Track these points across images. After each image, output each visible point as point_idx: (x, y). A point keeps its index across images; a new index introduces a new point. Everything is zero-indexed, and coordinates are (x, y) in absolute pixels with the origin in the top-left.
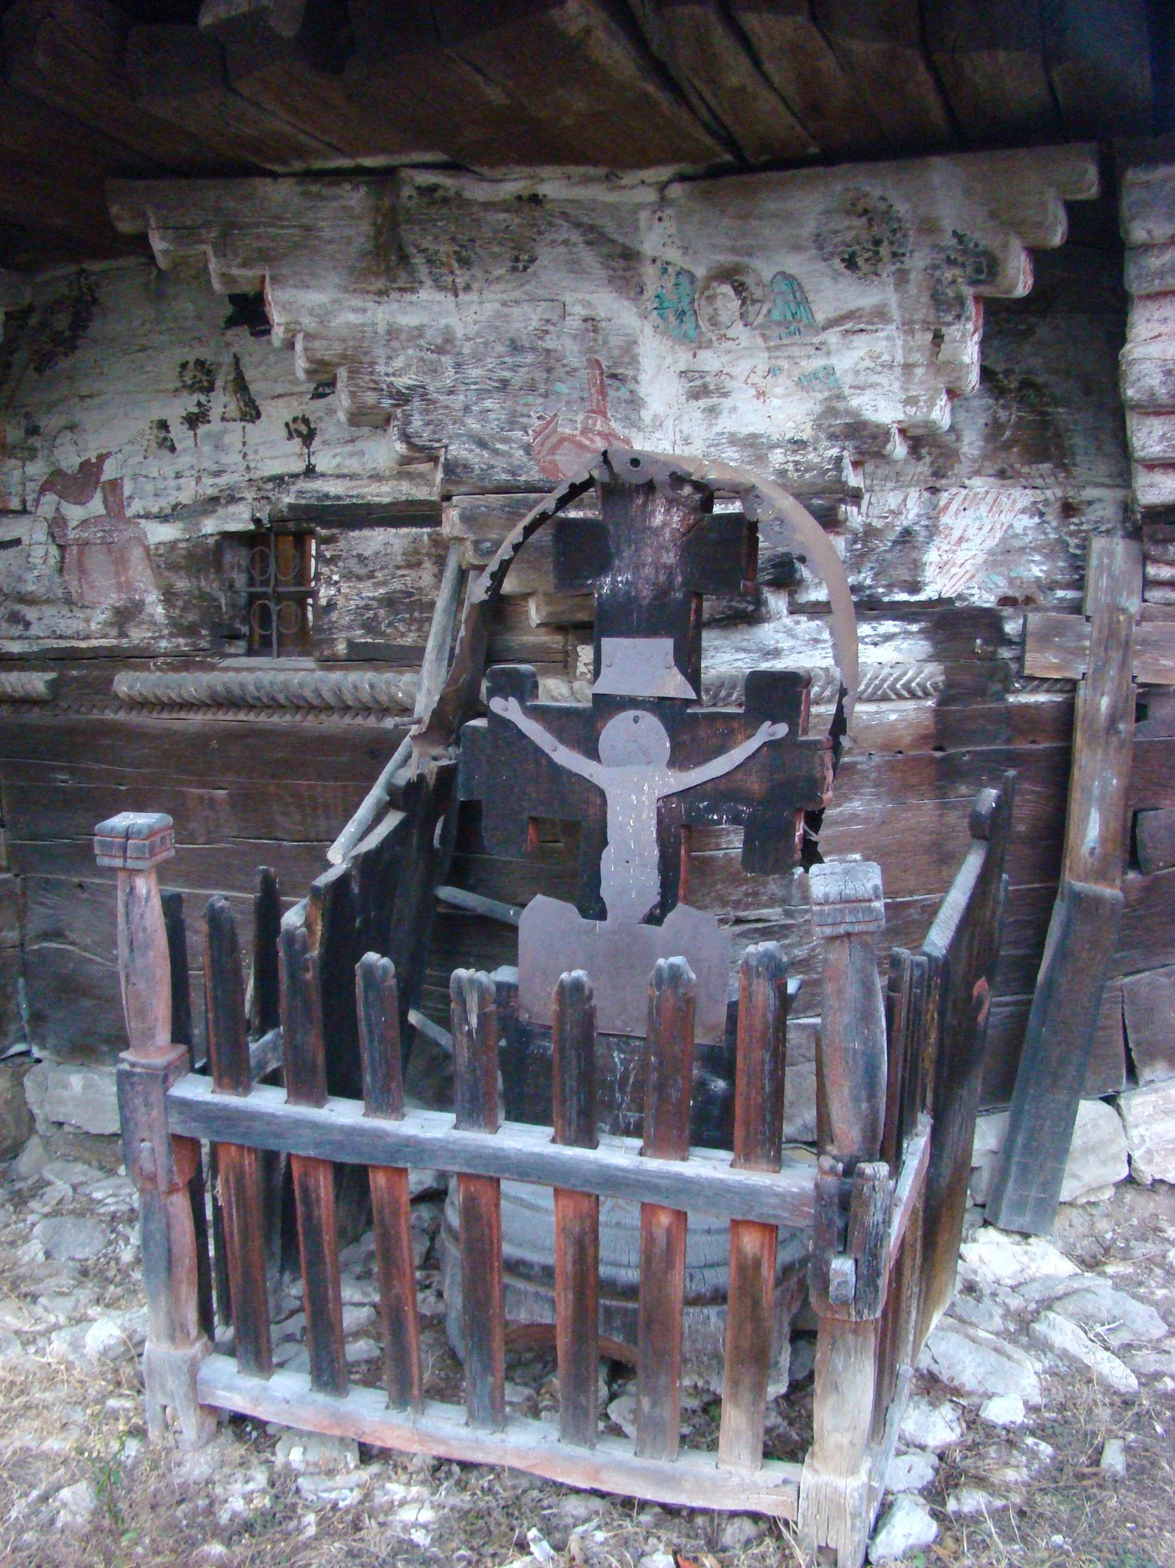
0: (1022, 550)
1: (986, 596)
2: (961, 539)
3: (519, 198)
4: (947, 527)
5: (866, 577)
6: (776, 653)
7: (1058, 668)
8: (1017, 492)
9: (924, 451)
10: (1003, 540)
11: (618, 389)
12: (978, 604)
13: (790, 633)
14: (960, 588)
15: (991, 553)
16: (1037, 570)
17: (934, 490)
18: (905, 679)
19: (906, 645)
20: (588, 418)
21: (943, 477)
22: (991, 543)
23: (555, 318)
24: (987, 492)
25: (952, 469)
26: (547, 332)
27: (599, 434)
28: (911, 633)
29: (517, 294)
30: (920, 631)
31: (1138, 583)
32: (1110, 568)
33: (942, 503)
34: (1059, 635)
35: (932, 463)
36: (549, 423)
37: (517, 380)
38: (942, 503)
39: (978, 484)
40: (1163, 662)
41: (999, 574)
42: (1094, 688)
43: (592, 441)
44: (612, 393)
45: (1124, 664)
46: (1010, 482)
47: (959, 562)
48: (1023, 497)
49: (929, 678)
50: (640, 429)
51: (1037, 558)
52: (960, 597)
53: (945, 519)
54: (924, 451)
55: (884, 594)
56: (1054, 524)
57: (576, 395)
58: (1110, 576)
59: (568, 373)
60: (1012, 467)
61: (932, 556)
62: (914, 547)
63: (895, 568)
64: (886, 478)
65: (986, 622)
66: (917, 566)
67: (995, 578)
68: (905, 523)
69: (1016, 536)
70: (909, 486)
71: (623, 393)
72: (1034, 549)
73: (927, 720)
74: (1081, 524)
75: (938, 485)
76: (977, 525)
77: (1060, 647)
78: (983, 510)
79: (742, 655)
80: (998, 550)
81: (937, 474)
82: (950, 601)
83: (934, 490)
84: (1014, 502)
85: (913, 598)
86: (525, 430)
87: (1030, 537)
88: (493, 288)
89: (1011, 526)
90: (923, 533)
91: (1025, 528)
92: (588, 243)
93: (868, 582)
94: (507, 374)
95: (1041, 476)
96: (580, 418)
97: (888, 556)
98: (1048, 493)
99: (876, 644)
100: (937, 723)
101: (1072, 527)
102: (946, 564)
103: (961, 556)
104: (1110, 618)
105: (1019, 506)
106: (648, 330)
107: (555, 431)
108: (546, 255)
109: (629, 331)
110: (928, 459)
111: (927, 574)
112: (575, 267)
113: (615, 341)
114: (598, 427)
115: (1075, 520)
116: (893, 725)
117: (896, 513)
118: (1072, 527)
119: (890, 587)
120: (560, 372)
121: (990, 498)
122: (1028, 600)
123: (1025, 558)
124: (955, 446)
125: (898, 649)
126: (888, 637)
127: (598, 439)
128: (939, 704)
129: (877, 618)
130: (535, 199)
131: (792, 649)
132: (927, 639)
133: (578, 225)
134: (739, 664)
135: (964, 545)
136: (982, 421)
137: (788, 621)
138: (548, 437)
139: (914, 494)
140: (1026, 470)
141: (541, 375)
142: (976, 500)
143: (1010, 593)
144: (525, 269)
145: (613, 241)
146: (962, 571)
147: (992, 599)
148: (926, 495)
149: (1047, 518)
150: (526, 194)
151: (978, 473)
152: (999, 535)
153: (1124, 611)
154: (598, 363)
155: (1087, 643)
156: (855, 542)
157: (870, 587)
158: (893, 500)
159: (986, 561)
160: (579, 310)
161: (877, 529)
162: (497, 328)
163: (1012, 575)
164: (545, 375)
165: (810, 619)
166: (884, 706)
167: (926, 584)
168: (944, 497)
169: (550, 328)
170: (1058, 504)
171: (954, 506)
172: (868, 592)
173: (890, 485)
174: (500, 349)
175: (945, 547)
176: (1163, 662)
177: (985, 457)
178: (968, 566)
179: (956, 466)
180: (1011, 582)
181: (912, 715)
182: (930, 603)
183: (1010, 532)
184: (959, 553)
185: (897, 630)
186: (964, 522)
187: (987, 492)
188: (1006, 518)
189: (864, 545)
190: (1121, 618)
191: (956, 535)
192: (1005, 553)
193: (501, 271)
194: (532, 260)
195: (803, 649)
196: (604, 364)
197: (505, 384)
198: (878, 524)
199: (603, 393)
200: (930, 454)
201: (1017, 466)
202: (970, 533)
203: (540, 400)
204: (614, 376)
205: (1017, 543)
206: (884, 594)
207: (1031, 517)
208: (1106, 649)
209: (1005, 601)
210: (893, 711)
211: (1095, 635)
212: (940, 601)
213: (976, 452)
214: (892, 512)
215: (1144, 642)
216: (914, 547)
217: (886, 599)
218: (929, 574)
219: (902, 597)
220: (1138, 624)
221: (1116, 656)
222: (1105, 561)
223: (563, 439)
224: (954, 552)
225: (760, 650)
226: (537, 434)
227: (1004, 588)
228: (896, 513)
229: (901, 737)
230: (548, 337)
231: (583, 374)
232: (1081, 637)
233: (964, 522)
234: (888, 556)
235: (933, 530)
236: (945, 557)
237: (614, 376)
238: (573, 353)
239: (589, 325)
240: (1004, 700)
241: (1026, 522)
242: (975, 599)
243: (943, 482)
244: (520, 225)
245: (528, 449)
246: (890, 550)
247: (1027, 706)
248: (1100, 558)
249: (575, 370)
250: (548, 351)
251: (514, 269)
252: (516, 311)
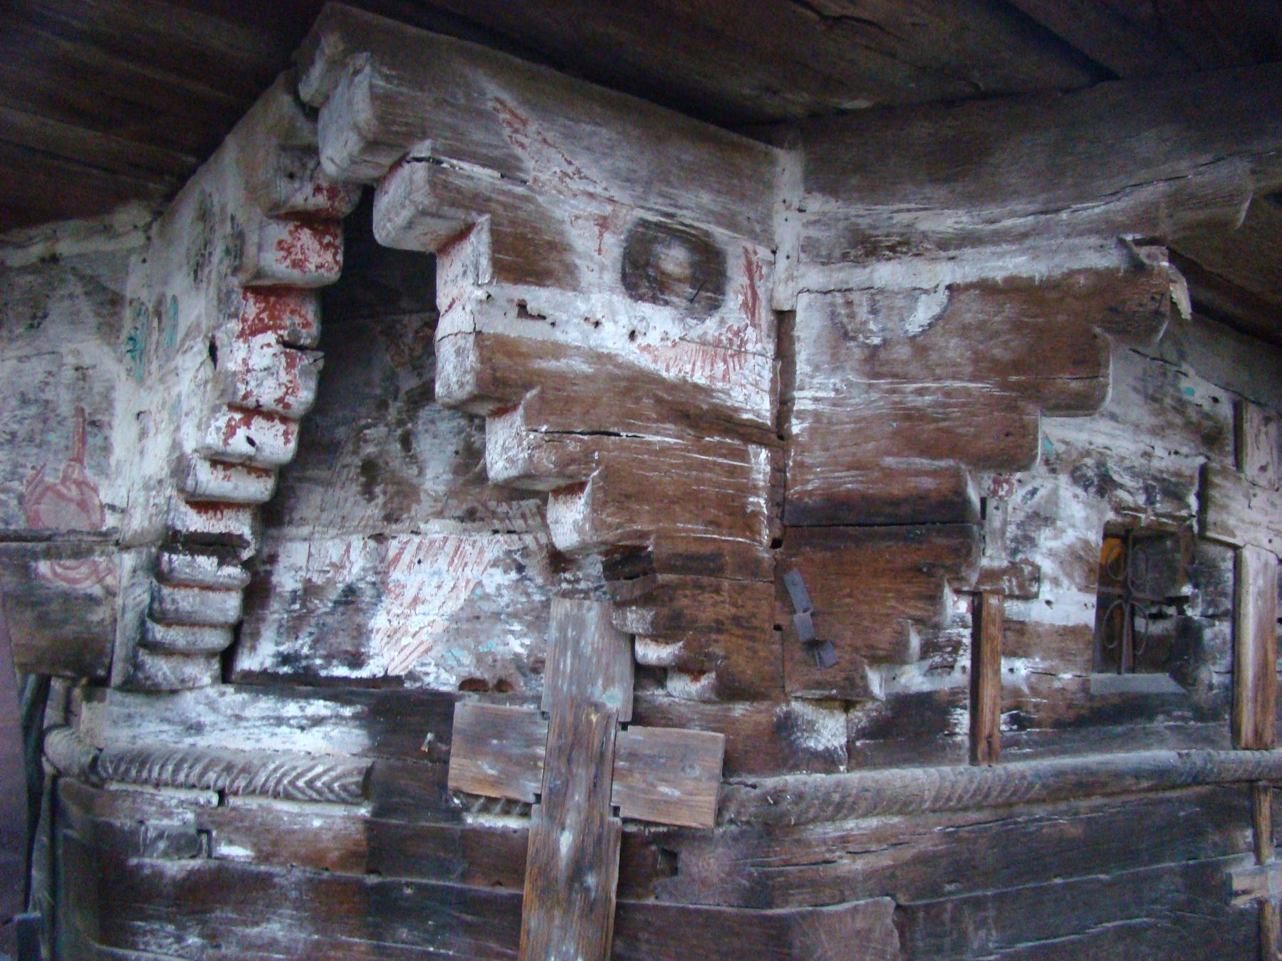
0: (496, 616)
1: (444, 676)
2: (416, 601)
3: (43, 260)
4: (398, 584)
5: (302, 645)
6: (198, 728)
7: (495, 782)
8: (484, 539)
9: (378, 490)
10: (470, 602)
11: (96, 435)
12: (434, 686)
13: (212, 705)
14: (412, 664)
15: (454, 618)
16: (517, 645)
17: (380, 538)
18: (310, 775)
19: (336, 732)
20: (69, 466)
21: (396, 521)
22: (453, 606)
23: (54, 369)
24: (446, 539)
25: (409, 509)
26: (47, 384)
27: (75, 482)
28: (342, 718)
29: (28, 350)
30: (355, 717)
31: (623, 669)
32: (577, 642)
33: (391, 554)
34: (500, 736)
35: (385, 504)
36: (39, 472)
37: (22, 431)
38: (391, 554)
39: (435, 529)
40: (664, 789)
41: (465, 648)
42: (551, 817)
43: (69, 489)
44: (90, 440)
45: (594, 788)
46: (477, 524)
47: (412, 631)
48: (495, 546)
49: (337, 778)
50: (107, 476)
51: (517, 627)
52: (411, 676)
53: (396, 575)
54: (378, 490)
55: (322, 667)
56: (540, 581)
57: (63, 443)
58: (577, 654)
59: (59, 423)
60: (485, 505)
61: (379, 621)
62: (358, 610)
63: (336, 635)
64: (331, 524)
65: (437, 707)
66: (361, 633)
67: (456, 652)
68: (349, 580)
69: (486, 597)
70: (351, 534)
71: (99, 441)
72: (515, 616)
73: (356, 831)
74: (578, 581)
75: (387, 532)
76: (434, 583)
77: (499, 755)
78: (442, 562)
79: (165, 727)
80: (463, 615)
81: (390, 518)
82: (398, 680)
83: (380, 538)
84: (481, 551)
85: (355, 674)
86: (21, 479)
87: (506, 600)
88: (14, 346)
89: (479, 584)
90: (370, 592)
91: (499, 587)
92: (87, 294)
93: (305, 651)
94: (15, 427)
95: (523, 516)
96: (62, 467)
97: (330, 620)
98: (528, 539)
99: (302, 728)
100: (369, 839)
101: (564, 586)
102: (396, 632)
103: (415, 622)
104: (576, 716)
105: (489, 556)
106: (123, 375)
107: (42, 481)
108: (57, 308)
109: (108, 376)
110: (381, 500)
111: (372, 644)
112: (74, 319)
113: (98, 387)
114: (75, 476)
115: (568, 576)
116: (317, 833)
117: (338, 567)
118: (564, 586)
119: (329, 658)
120: (53, 423)
121: (450, 548)
122: (502, 685)
123: (499, 627)
124: (415, 481)
125: (326, 737)
126: (317, 721)
127: (73, 487)
128: (375, 813)
129: (307, 696)
130: (54, 259)
131: (214, 724)
132: (361, 727)
133: (82, 278)
134: (164, 736)
135: (420, 608)
136: (452, 448)
137: (212, 692)
138: (36, 486)
139: (357, 542)
140: (504, 508)
141: (39, 426)
142: (433, 549)
143: (478, 675)
144: (39, 324)
145: (105, 289)
146: (415, 642)
147: (453, 680)
148: (372, 544)
149: (529, 572)
150: (47, 256)
151: (440, 514)
152: (464, 595)
153: (597, 707)
154: (83, 410)
155: (541, 751)
156: (294, 602)
157: (307, 657)
158: (334, 550)
159: (446, 630)
160: (70, 360)
161: (318, 587)
162: (13, 383)
163: (481, 649)
164: (41, 426)
165: (238, 691)
166: (309, 808)
167: (370, 657)
168: (393, 546)
169: (51, 380)
170: (544, 553)
171: (406, 558)
172: (304, 663)
173: (332, 532)
174: (14, 402)
175: (396, 610)
176: (664, 789)
177: (452, 494)
178: (423, 636)
179: (414, 507)
180: (480, 659)
181: (339, 824)
182: (373, 681)
183: (479, 591)
184: (414, 618)
185: (327, 712)
186: (420, 578)
187: (446, 539)
188: (472, 573)
189: (303, 605)
190: (594, 718)
191: (410, 594)
192: (472, 620)
193: (21, 330)
194: (45, 316)
195: (224, 725)
196: (87, 411)
197: (13, 435)
198: (318, 579)
199: (83, 441)
200: (385, 493)
201: (492, 504)
202: (427, 592)
203: (36, 450)
204: (93, 423)
205: (486, 607)
206: (322, 667)
207: (505, 572)
208: (569, 761)
209: (470, 684)
210: (318, 815)
211: (552, 740)
212: (387, 679)
213: (441, 489)
214: (332, 565)
215: (632, 756)
216: (358, 610)
217: (323, 673)
218: (376, 643)
219: (341, 671)
220: (624, 726)
221: (583, 774)
222: (570, 633)
223: (48, 489)
224: (407, 617)
225: (182, 723)
226: (29, 483)
227: (469, 666)
228: (338, 567)
229: (328, 850)
230: (47, 389)
231: (70, 423)
232: (532, 741)
233: (420, 578)
234: (330, 620)
235: (380, 588)
236: (395, 623)
237: (93, 423)
238: (65, 403)
239: (79, 374)
240: (460, 820)
241: (498, 579)
242: (430, 679)
243: (394, 527)
244: (40, 285)
245: (21, 498)
246: (332, 612)
247: (490, 832)
248: (562, 629)
249: (65, 419)
250: (47, 402)
251: (31, 326)
252: (27, 366)
